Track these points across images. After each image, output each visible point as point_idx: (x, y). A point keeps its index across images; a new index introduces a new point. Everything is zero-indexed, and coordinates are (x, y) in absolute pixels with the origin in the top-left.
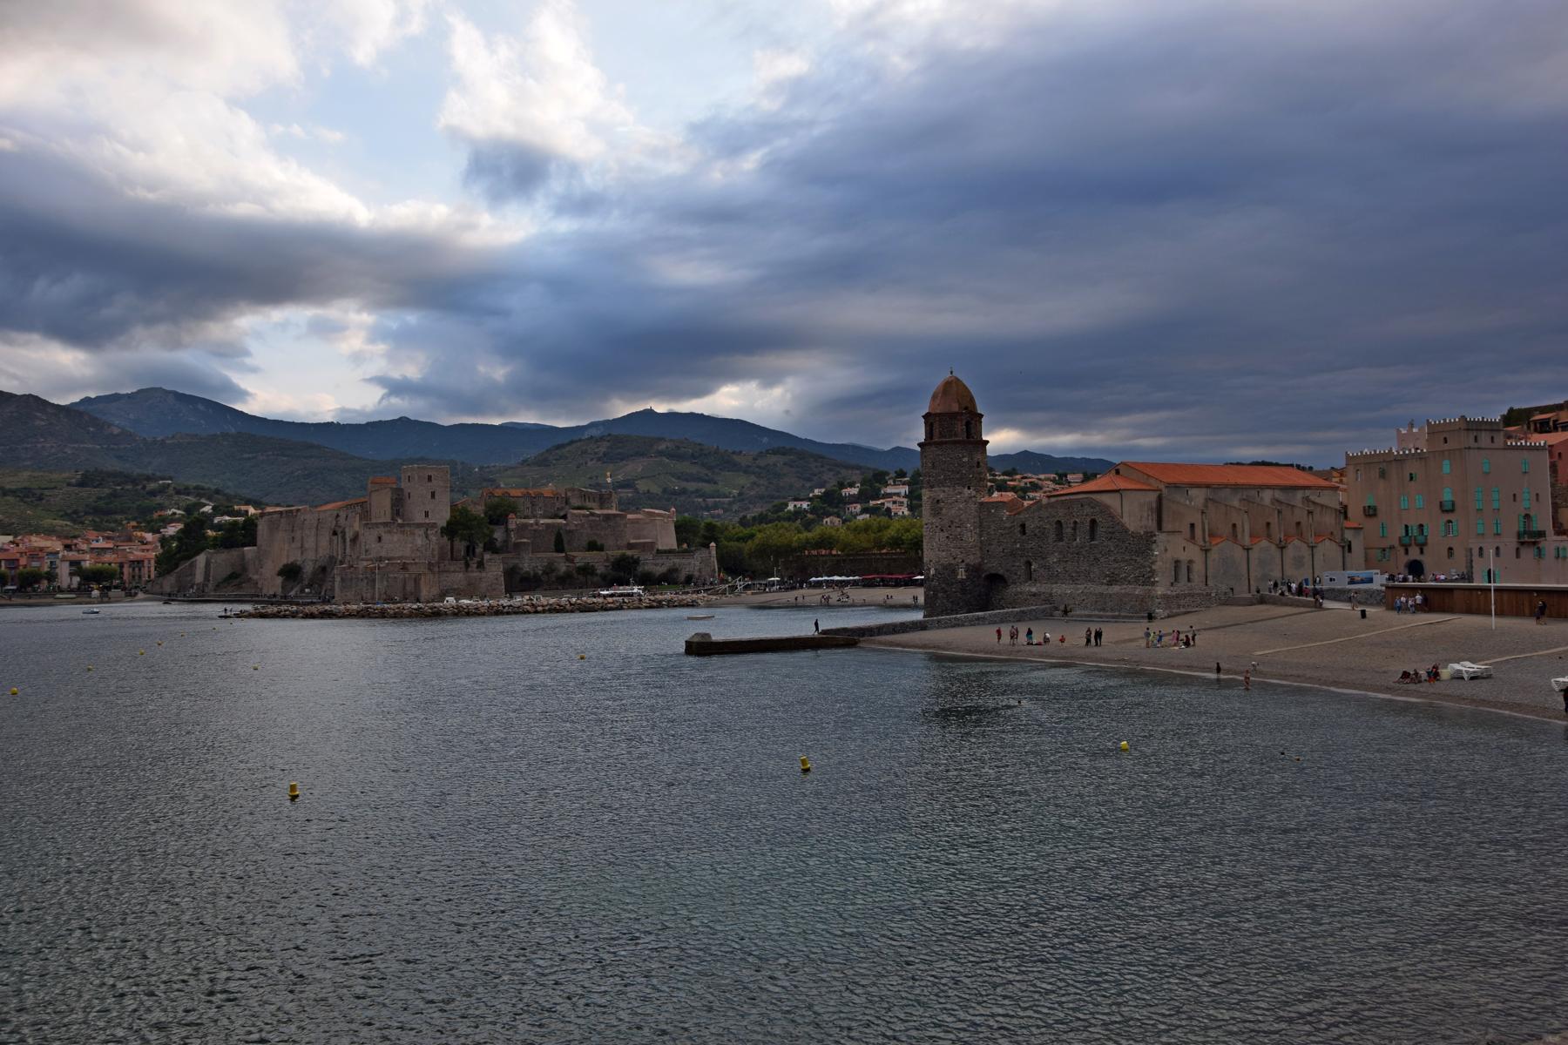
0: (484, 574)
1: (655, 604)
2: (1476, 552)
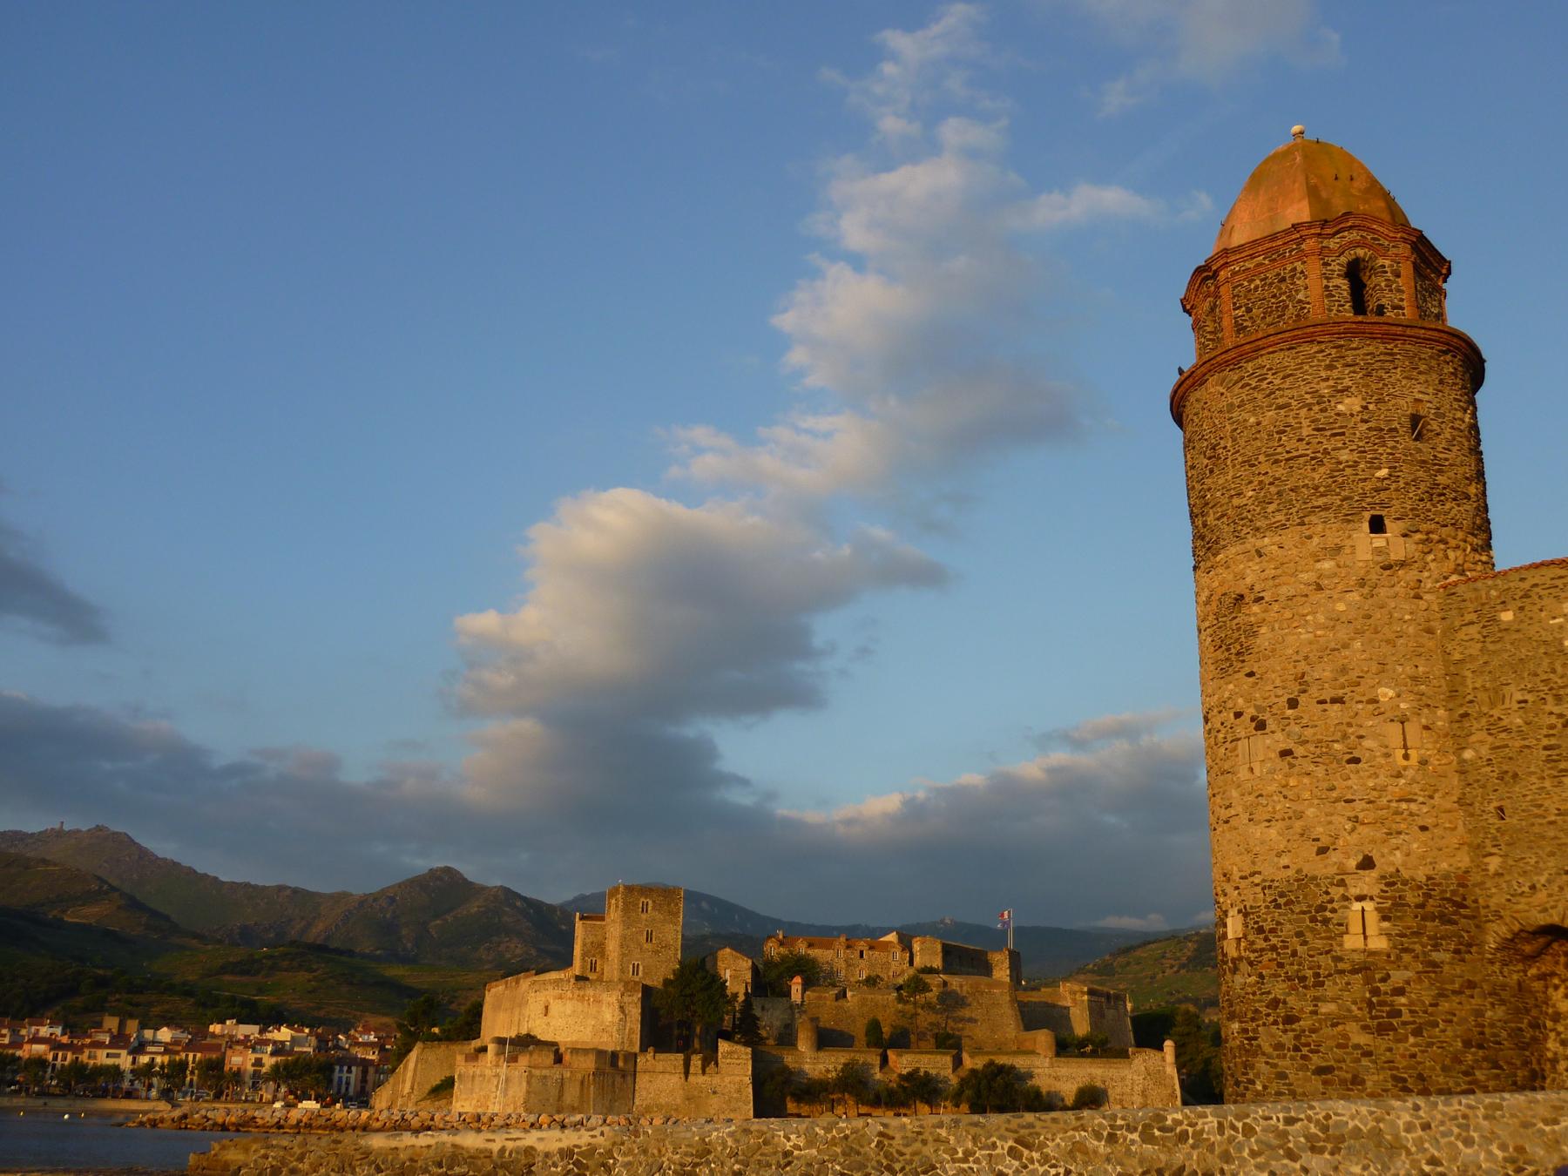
0: (716, 1080)
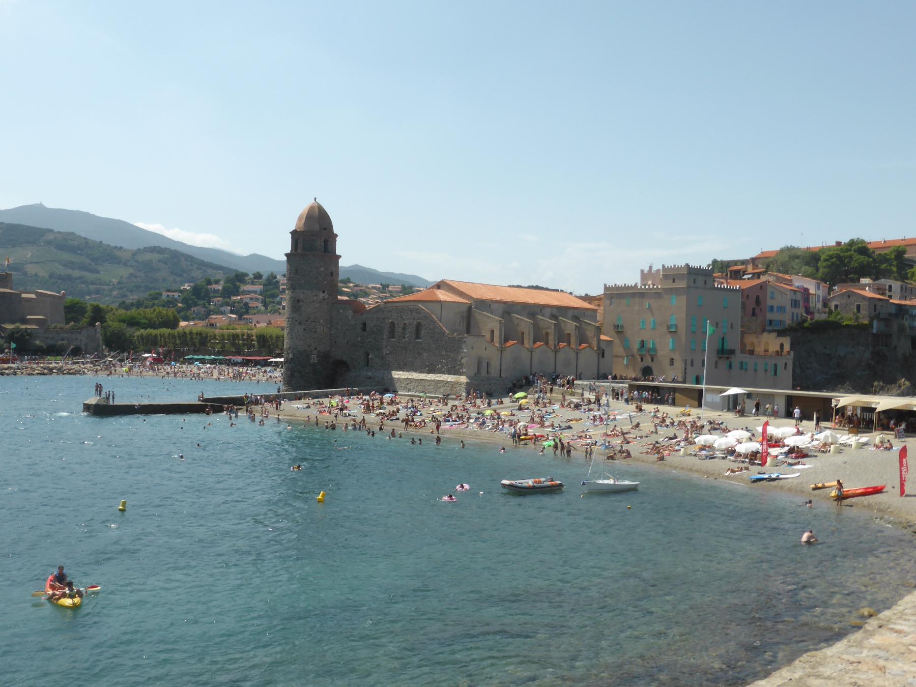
1: (46, 371)
2: (689, 363)
